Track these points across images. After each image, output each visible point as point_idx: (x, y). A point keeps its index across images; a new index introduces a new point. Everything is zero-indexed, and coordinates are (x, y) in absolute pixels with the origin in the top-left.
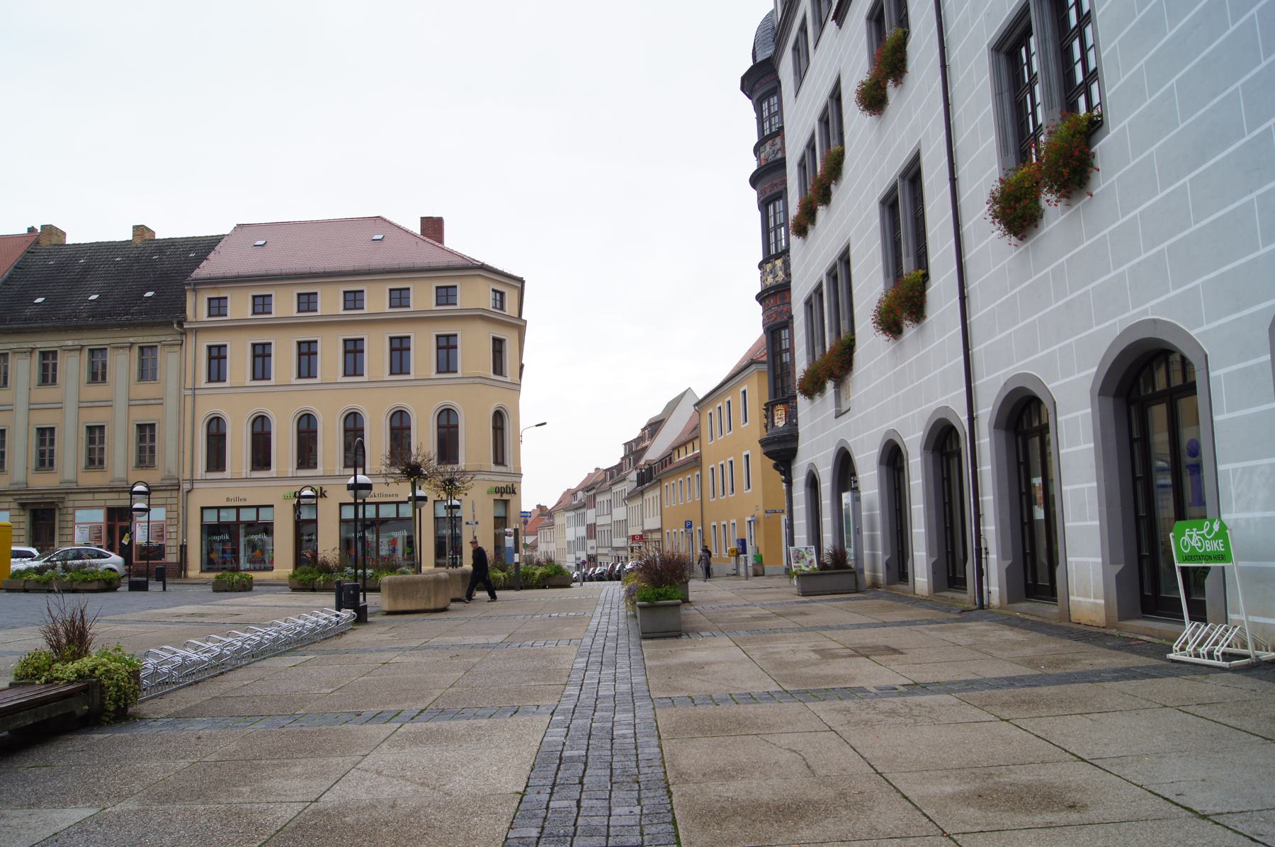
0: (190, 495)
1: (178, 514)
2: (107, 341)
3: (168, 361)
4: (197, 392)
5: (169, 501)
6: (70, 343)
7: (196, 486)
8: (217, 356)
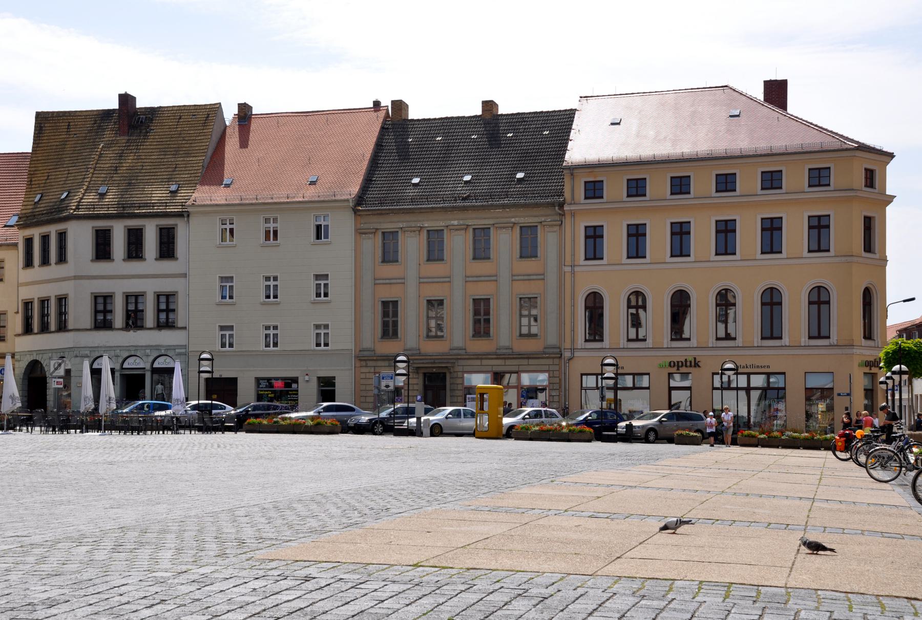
0: (571, 362)
1: (560, 380)
2: (491, 222)
3: (548, 240)
4: (576, 269)
5: (552, 368)
6: (456, 223)
7: (576, 354)
8: (594, 236)
